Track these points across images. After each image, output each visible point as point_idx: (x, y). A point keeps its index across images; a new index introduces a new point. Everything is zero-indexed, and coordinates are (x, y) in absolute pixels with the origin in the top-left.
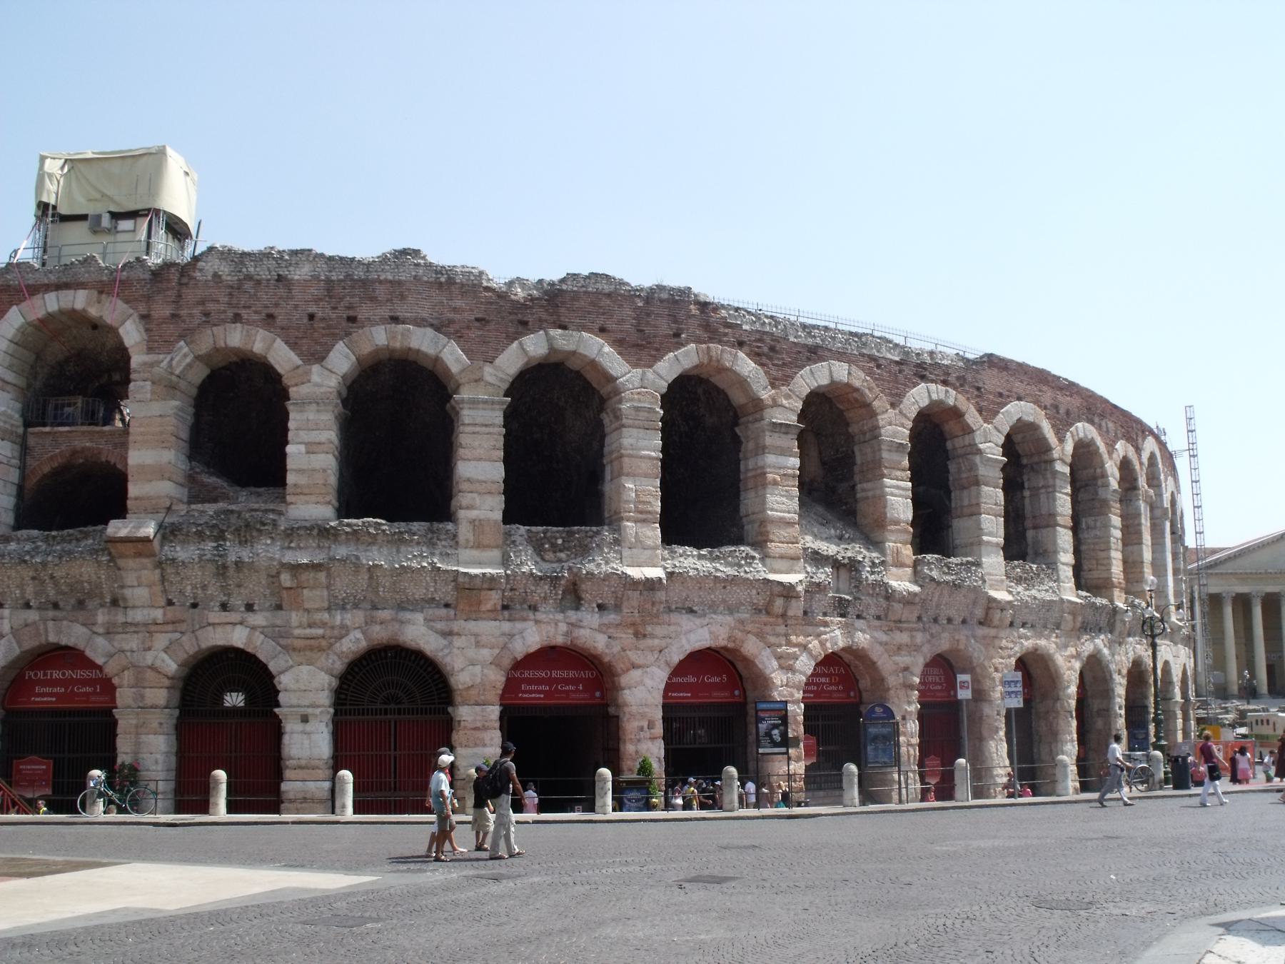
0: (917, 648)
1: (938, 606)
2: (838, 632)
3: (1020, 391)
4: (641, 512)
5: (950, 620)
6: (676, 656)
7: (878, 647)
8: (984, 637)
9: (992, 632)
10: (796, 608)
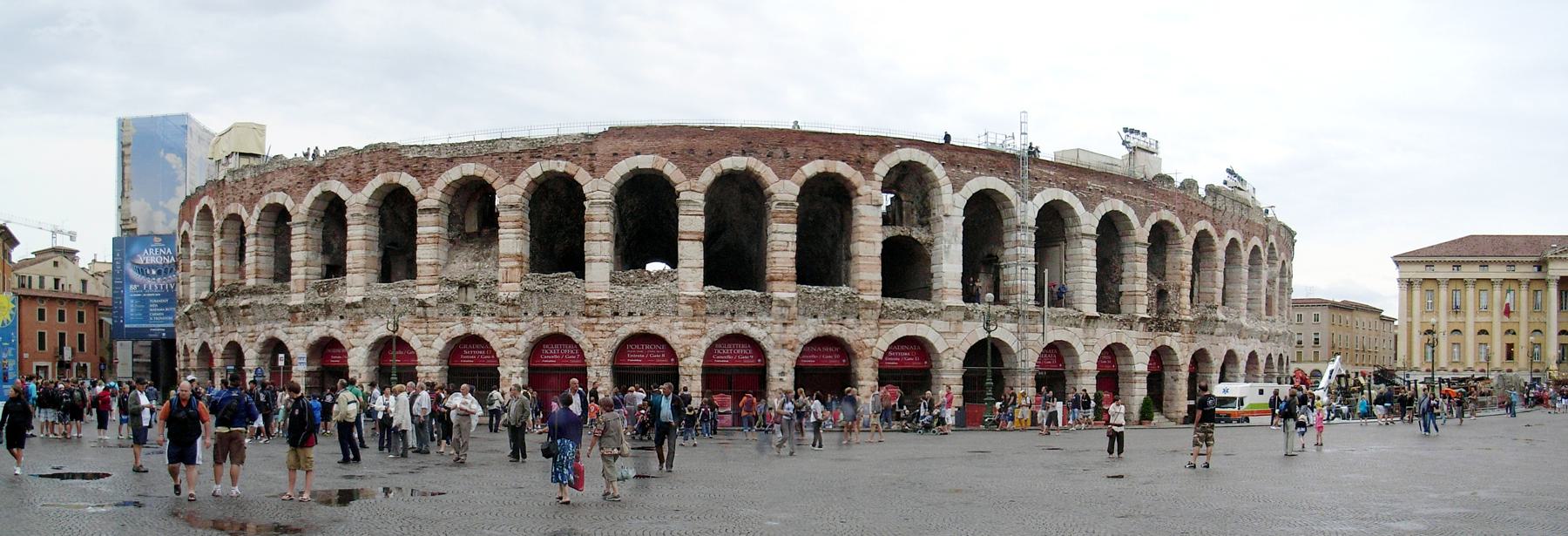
0: (520, 333)
9: (593, 320)
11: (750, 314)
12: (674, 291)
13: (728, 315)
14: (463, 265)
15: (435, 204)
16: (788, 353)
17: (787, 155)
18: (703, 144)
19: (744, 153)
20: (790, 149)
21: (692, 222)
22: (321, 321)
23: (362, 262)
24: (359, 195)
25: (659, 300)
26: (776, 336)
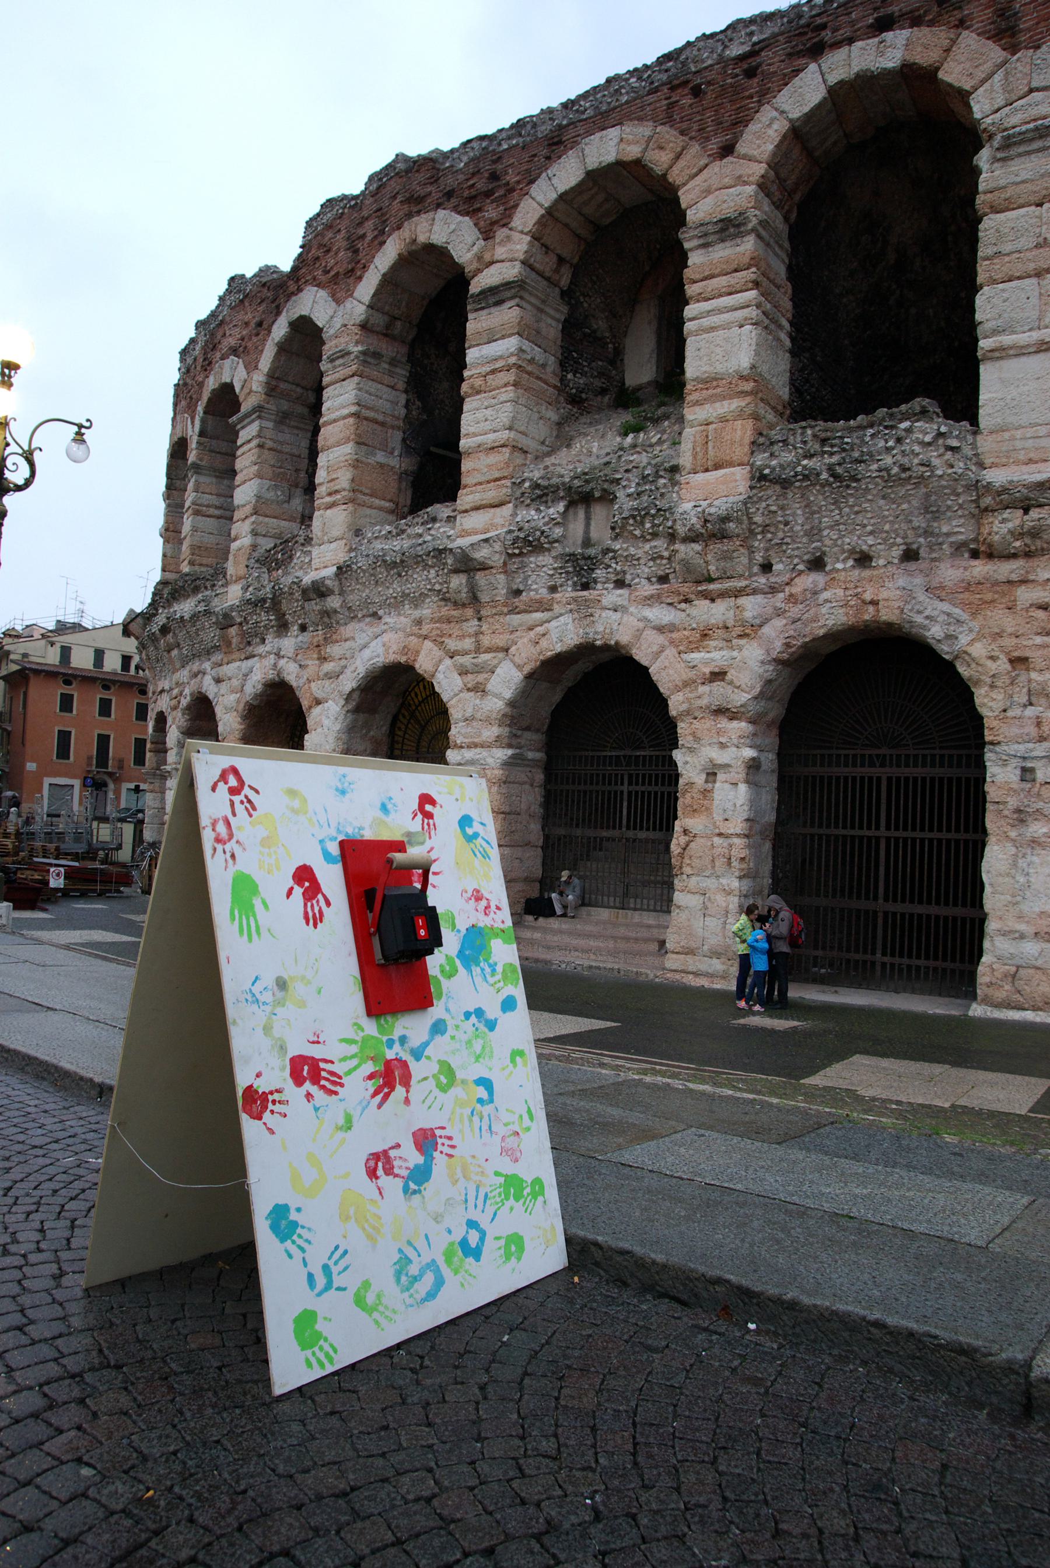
0: (749, 631)
1: (814, 533)
2: (567, 619)
4: (330, 494)
5: (863, 560)
6: (349, 682)
7: (650, 635)
8: (968, 587)
9: (1006, 569)
10: (494, 586)
14: (595, 447)
15: (510, 271)
22: (272, 642)
23: (344, 479)
24: (349, 304)
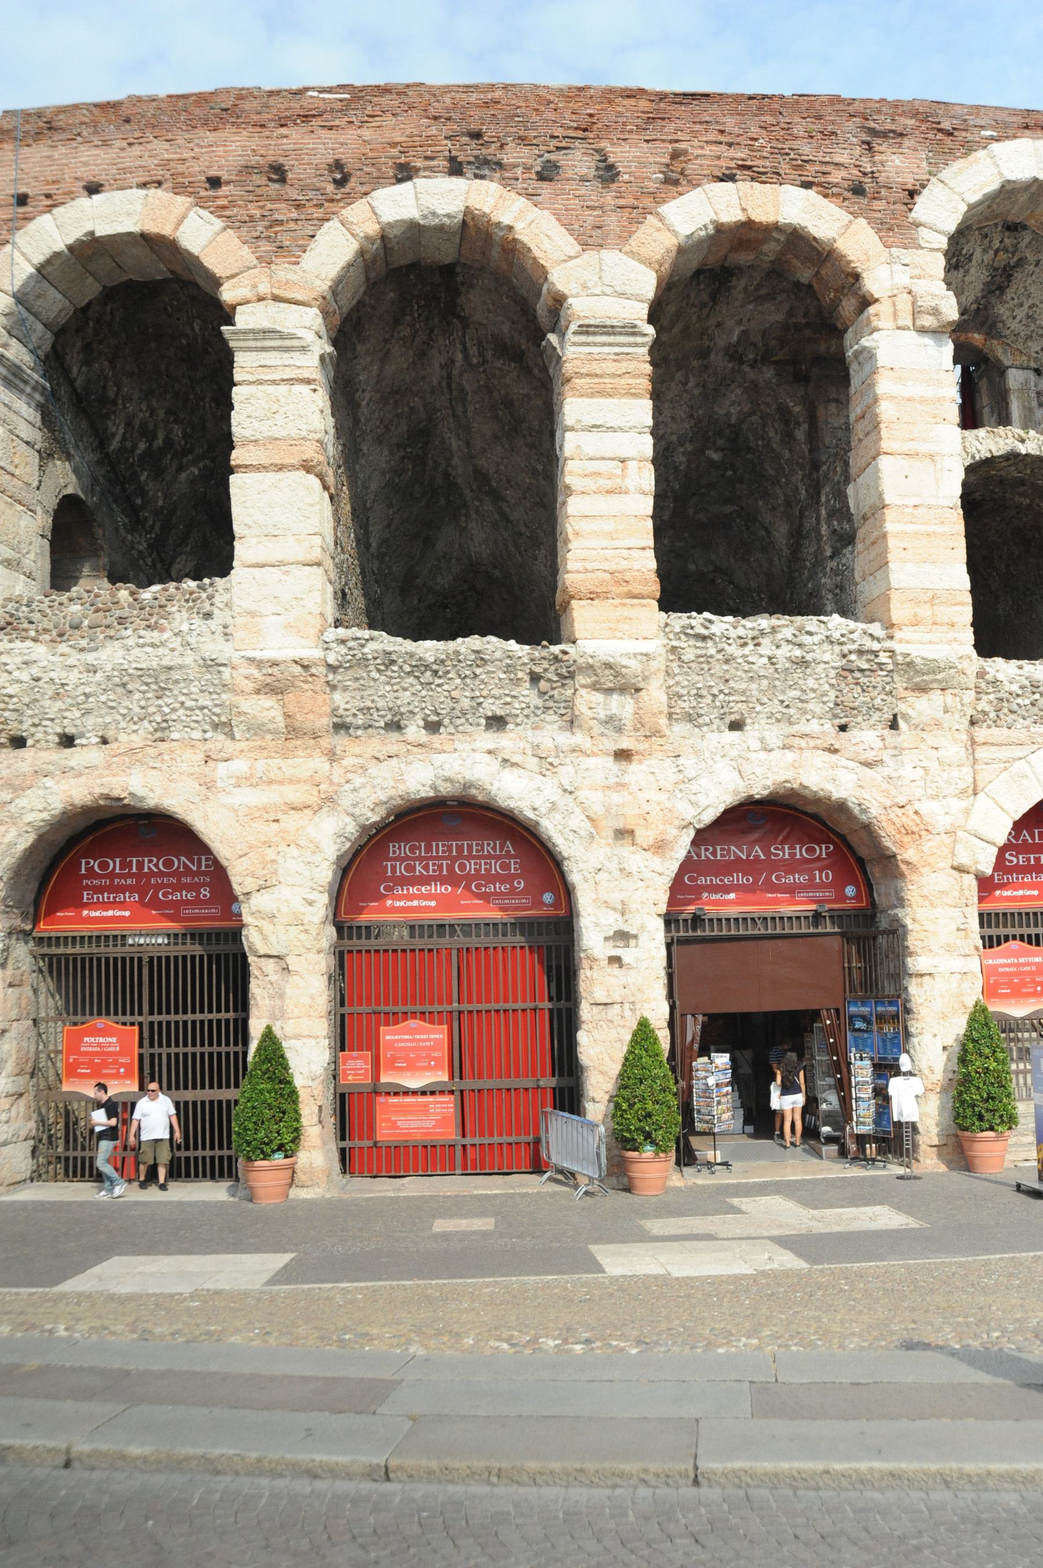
3: (89, 174)
11: (497, 722)
12: (216, 648)
13: (414, 731)
16: (636, 860)
17: (608, 173)
18: (310, 150)
19: (456, 169)
20: (621, 154)
21: (281, 409)
25: (159, 680)
26: (595, 800)
